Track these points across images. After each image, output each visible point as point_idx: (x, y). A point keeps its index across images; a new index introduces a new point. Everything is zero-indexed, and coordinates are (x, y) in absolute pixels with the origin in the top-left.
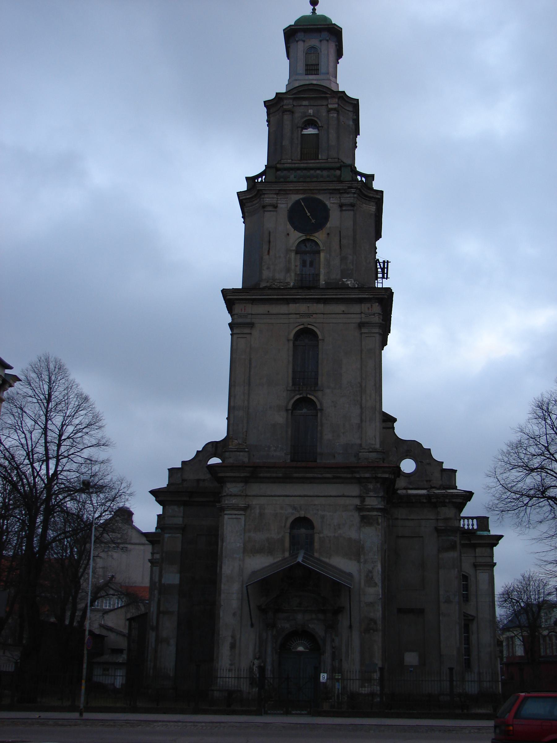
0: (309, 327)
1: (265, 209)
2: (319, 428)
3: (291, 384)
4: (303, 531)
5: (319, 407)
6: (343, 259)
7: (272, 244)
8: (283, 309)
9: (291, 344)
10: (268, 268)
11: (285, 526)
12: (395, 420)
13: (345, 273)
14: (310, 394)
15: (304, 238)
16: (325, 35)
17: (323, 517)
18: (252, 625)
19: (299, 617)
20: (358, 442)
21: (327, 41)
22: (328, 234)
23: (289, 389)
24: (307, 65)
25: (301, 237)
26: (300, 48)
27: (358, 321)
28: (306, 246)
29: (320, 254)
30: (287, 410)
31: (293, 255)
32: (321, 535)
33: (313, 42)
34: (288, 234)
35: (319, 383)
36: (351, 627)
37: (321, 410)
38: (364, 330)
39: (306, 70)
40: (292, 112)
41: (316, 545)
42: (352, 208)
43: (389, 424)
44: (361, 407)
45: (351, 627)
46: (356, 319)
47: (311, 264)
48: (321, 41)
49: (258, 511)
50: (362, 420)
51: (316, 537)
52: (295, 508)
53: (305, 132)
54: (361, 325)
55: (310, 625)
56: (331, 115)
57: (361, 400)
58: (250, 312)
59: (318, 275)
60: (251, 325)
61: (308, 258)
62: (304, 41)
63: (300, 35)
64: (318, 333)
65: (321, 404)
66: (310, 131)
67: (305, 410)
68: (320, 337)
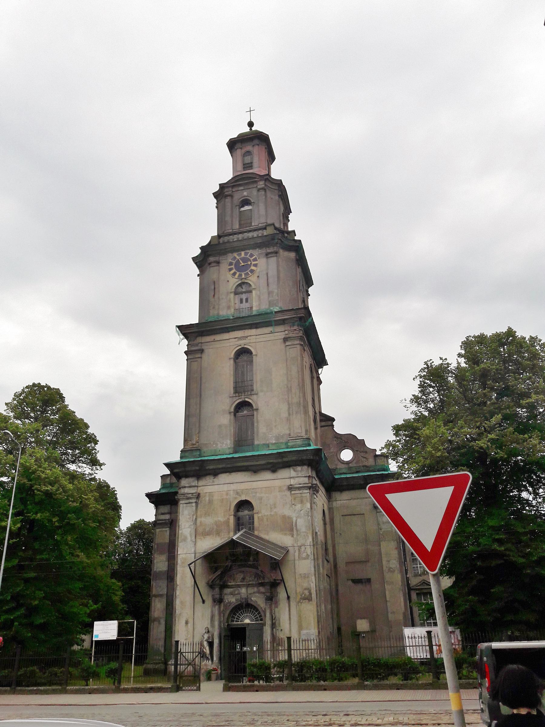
0: (245, 346)
1: (211, 266)
2: (255, 424)
3: (232, 392)
4: (246, 512)
5: (255, 407)
6: (270, 293)
7: (216, 290)
8: (226, 336)
9: (232, 361)
10: (214, 308)
11: (230, 509)
12: (333, 420)
13: (271, 304)
14: (247, 398)
15: (240, 282)
16: (256, 141)
17: (261, 499)
18: (204, 602)
19: (243, 590)
20: (288, 432)
21: (258, 145)
22: (258, 276)
23: (231, 396)
24: (244, 164)
25: (237, 282)
26: (239, 153)
27: (283, 337)
28: (242, 288)
29: (252, 292)
30: (230, 413)
31: (232, 295)
32: (260, 515)
33: (249, 148)
34: (228, 281)
35: (255, 388)
36: (288, 598)
37: (257, 409)
38: (287, 343)
39: (244, 168)
40: (231, 196)
41: (256, 523)
42: (275, 255)
43: (330, 423)
44: (289, 404)
45: (288, 598)
46: (282, 335)
47: (247, 300)
48: (253, 146)
49: (207, 499)
50: (289, 414)
51: (256, 517)
52: (237, 493)
53: (242, 209)
54: (285, 340)
55: (252, 599)
56: (260, 193)
57: (288, 398)
58: (200, 341)
59: (251, 308)
60: (202, 351)
61: (244, 296)
62: (241, 148)
63: (238, 145)
64: (253, 350)
65: (256, 404)
66: (246, 208)
67: (245, 412)
68: (254, 353)
